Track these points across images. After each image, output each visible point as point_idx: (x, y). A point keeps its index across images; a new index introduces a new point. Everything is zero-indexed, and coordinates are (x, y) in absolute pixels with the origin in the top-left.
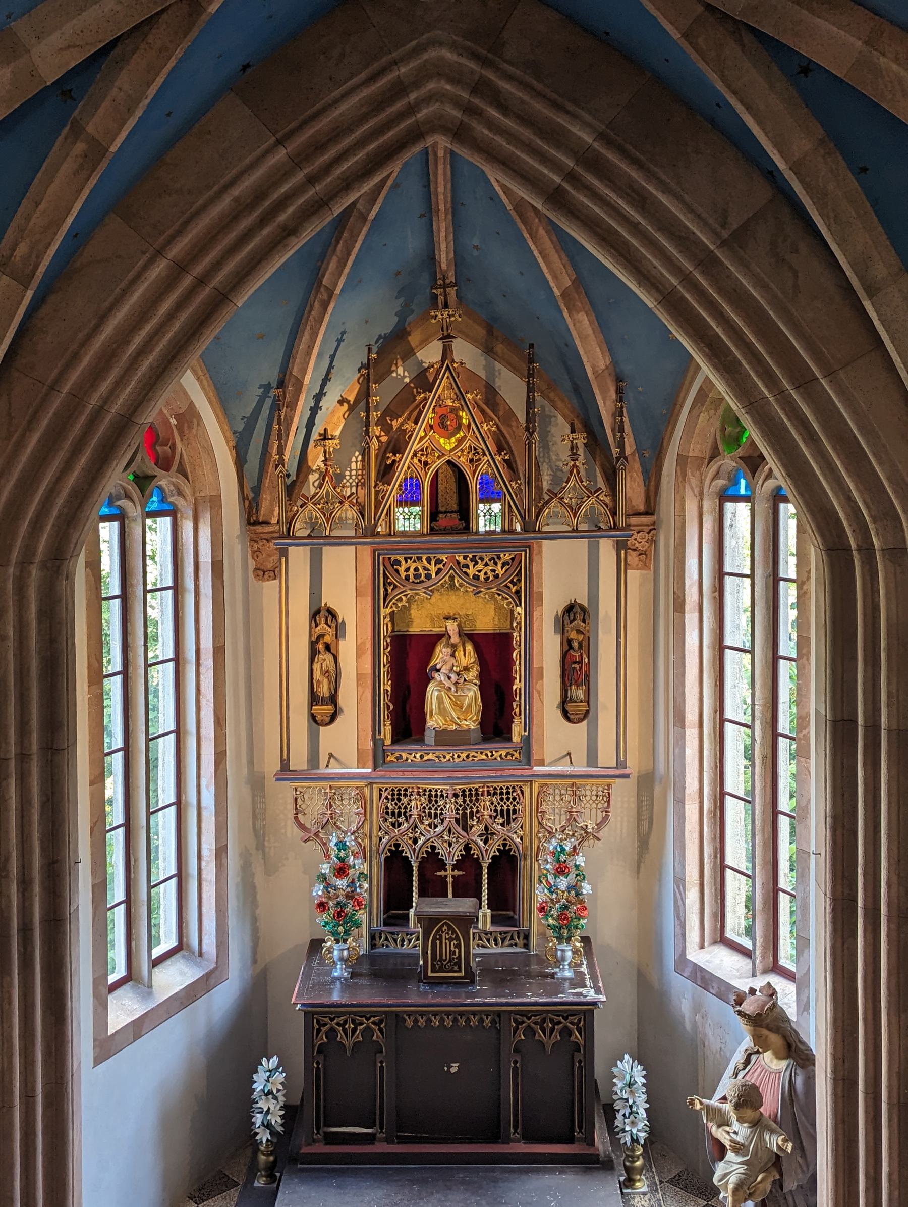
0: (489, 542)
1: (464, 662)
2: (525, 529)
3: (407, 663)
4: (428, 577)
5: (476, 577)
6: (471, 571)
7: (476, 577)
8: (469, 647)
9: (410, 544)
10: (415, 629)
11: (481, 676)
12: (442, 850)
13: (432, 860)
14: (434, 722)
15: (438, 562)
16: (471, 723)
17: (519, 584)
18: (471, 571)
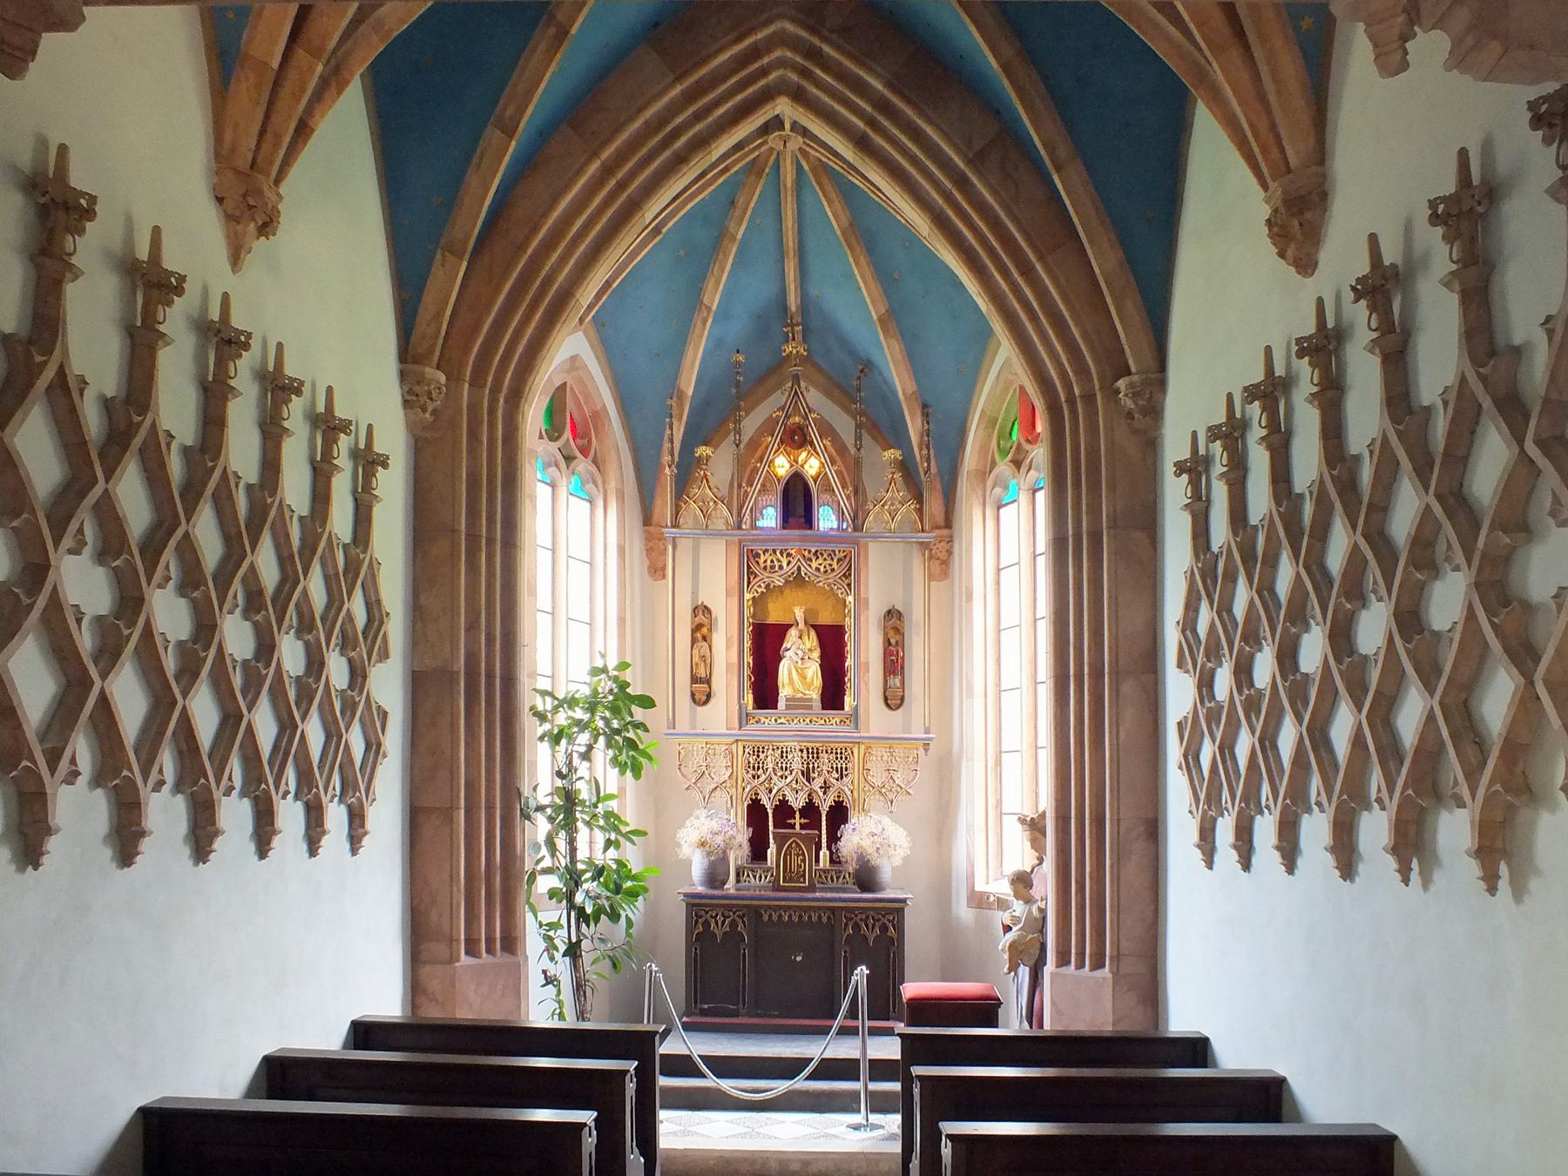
0: (825, 538)
1: (808, 645)
2: (855, 529)
3: (766, 644)
4: (781, 567)
5: (818, 569)
6: (814, 564)
7: (818, 569)
8: (813, 634)
9: (767, 537)
10: (771, 620)
11: (822, 657)
12: (790, 798)
13: (784, 810)
14: (784, 692)
15: (789, 555)
16: (815, 695)
17: (849, 573)
18: (814, 564)
